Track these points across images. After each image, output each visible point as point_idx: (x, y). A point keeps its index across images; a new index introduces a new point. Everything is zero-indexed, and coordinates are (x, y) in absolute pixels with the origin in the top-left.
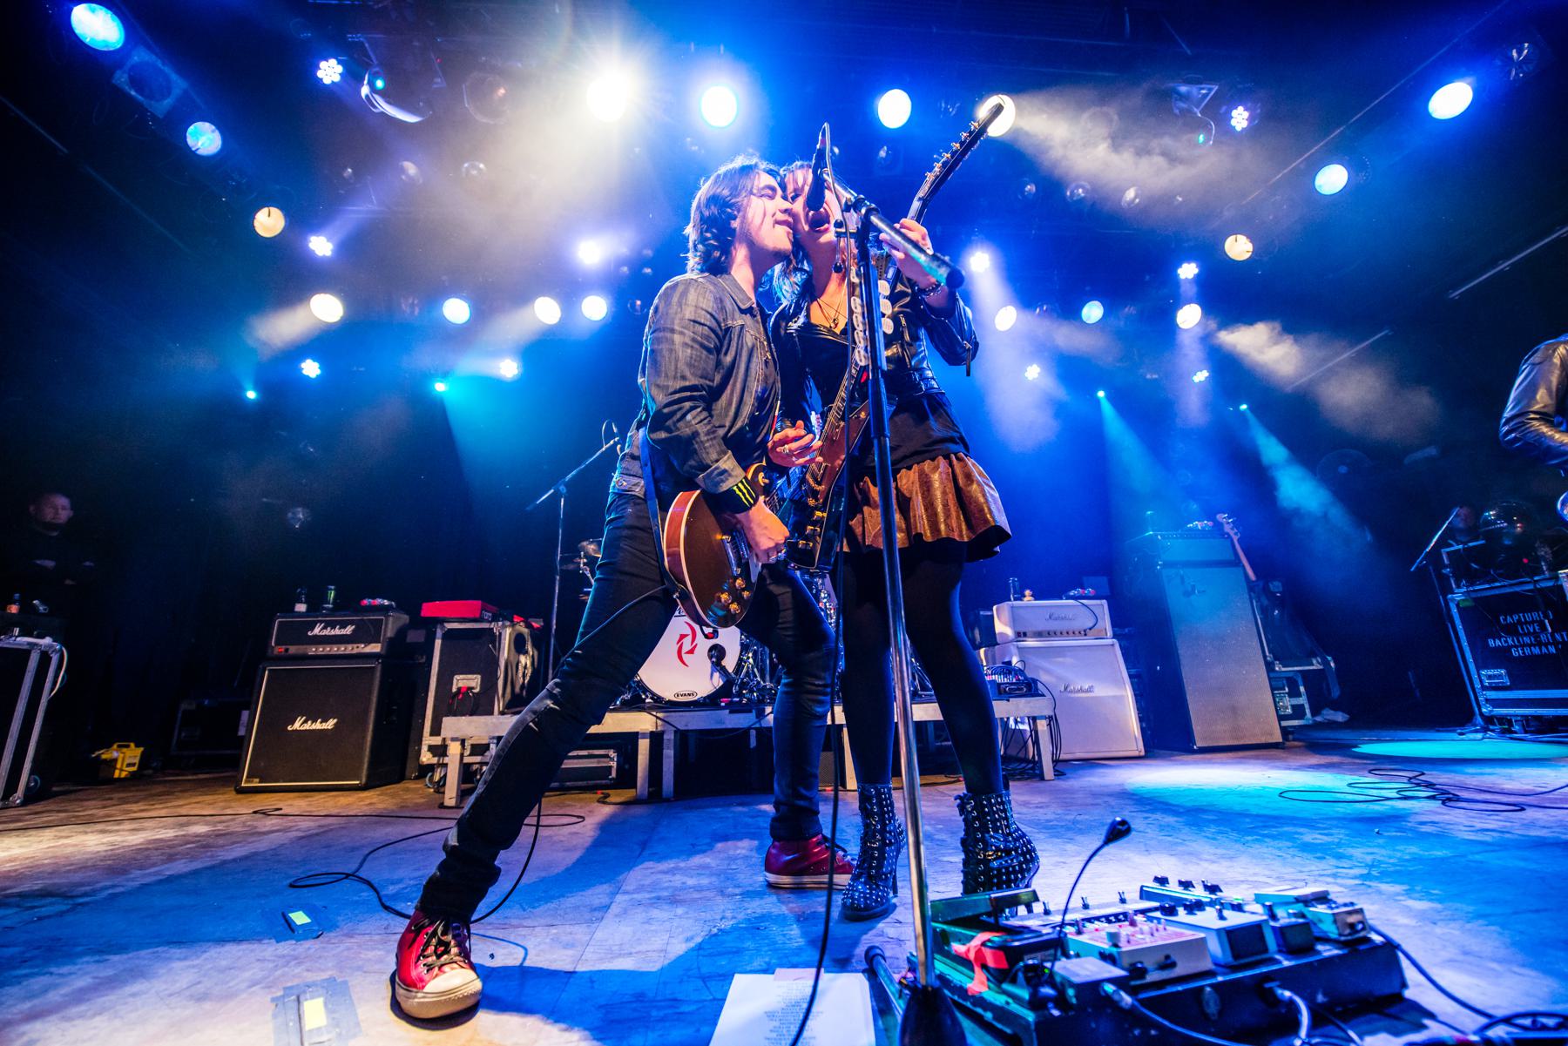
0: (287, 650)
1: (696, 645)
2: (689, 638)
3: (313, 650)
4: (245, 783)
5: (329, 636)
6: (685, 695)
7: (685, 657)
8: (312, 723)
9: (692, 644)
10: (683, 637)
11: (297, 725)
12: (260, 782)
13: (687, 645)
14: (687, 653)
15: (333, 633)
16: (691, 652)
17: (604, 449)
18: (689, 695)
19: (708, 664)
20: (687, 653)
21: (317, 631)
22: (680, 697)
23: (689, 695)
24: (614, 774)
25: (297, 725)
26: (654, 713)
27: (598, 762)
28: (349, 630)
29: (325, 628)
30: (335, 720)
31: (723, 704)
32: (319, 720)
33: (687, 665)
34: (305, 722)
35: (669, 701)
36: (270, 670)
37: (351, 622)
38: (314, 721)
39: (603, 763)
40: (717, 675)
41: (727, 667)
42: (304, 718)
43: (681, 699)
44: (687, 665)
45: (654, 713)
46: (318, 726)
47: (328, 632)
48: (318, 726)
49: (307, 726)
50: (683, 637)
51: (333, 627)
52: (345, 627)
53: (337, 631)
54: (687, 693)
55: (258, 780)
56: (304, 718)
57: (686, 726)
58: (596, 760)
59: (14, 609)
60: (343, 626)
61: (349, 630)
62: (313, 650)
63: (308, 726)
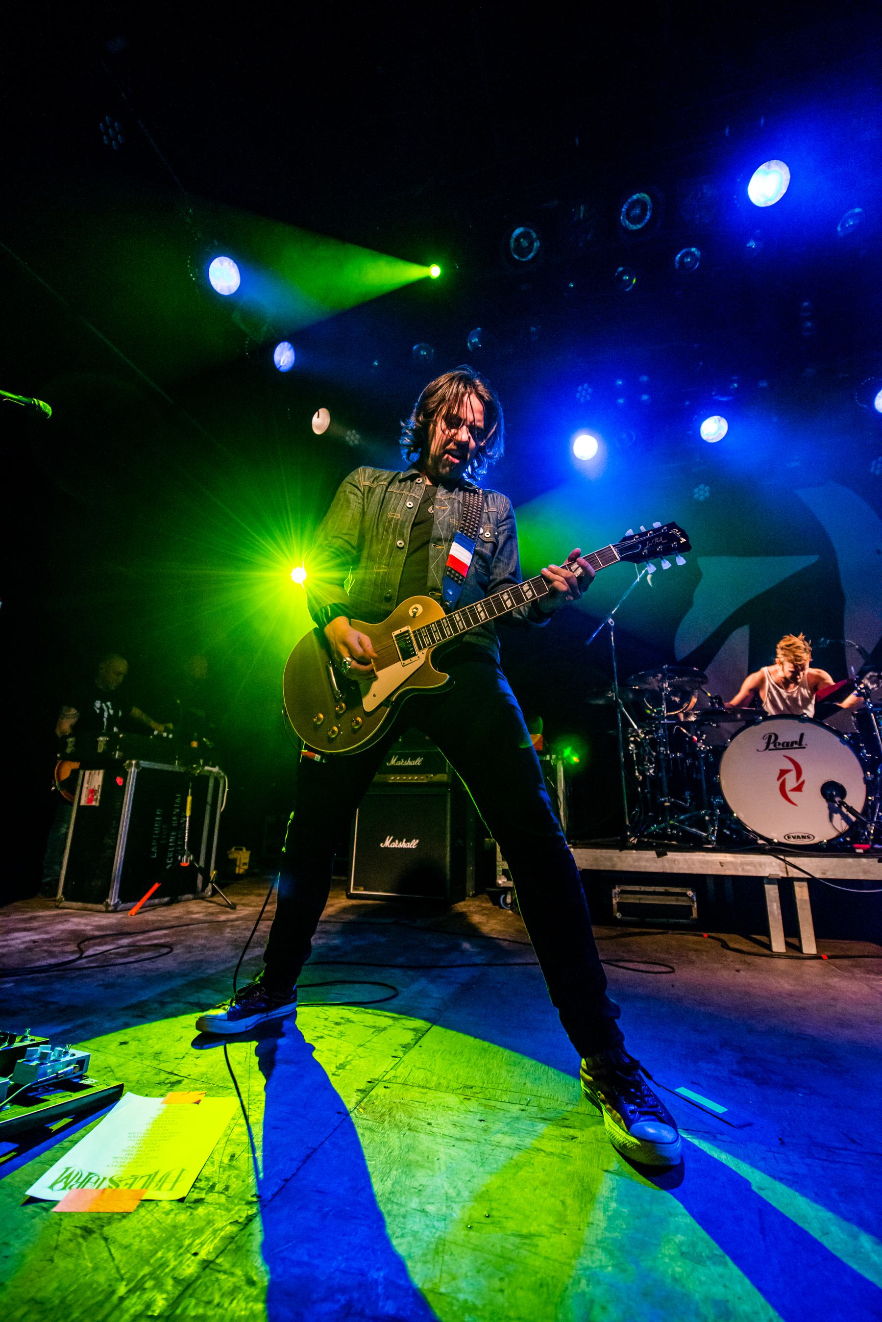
3: (392, 778)
4: (355, 889)
6: (798, 837)
7: (792, 795)
8: (399, 842)
10: (783, 772)
11: (387, 843)
12: (365, 890)
13: (791, 781)
14: (794, 790)
16: (799, 789)
17: (638, 580)
18: (804, 837)
19: (823, 804)
21: (393, 762)
22: (792, 839)
23: (804, 837)
24: (695, 914)
25: (387, 843)
26: (782, 857)
27: (677, 900)
28: (418, 762)
29: (399, 760)
31: (860, 851)
32: (405, 840)
34: (393, 841)
35: (780, 844)
38: (401, 840)
39: (682, 902)
40: (837, 817)
41: (854, 807)
43: (792, 841)
45: (782, 857)
46: (403, 845)
47: (401, 763)
48: (403, 845)
49: (395, 845)
50: (783, 772)
51: (406, 759)
52: (415, 759)
53: (409, 763)
54: (800, 835)
55: (362, 888)
57: (824, 873)
58: (673, 898)
59: (195, 744)
60: (414, 758)
61: (418, 762)
62: (392, 778)
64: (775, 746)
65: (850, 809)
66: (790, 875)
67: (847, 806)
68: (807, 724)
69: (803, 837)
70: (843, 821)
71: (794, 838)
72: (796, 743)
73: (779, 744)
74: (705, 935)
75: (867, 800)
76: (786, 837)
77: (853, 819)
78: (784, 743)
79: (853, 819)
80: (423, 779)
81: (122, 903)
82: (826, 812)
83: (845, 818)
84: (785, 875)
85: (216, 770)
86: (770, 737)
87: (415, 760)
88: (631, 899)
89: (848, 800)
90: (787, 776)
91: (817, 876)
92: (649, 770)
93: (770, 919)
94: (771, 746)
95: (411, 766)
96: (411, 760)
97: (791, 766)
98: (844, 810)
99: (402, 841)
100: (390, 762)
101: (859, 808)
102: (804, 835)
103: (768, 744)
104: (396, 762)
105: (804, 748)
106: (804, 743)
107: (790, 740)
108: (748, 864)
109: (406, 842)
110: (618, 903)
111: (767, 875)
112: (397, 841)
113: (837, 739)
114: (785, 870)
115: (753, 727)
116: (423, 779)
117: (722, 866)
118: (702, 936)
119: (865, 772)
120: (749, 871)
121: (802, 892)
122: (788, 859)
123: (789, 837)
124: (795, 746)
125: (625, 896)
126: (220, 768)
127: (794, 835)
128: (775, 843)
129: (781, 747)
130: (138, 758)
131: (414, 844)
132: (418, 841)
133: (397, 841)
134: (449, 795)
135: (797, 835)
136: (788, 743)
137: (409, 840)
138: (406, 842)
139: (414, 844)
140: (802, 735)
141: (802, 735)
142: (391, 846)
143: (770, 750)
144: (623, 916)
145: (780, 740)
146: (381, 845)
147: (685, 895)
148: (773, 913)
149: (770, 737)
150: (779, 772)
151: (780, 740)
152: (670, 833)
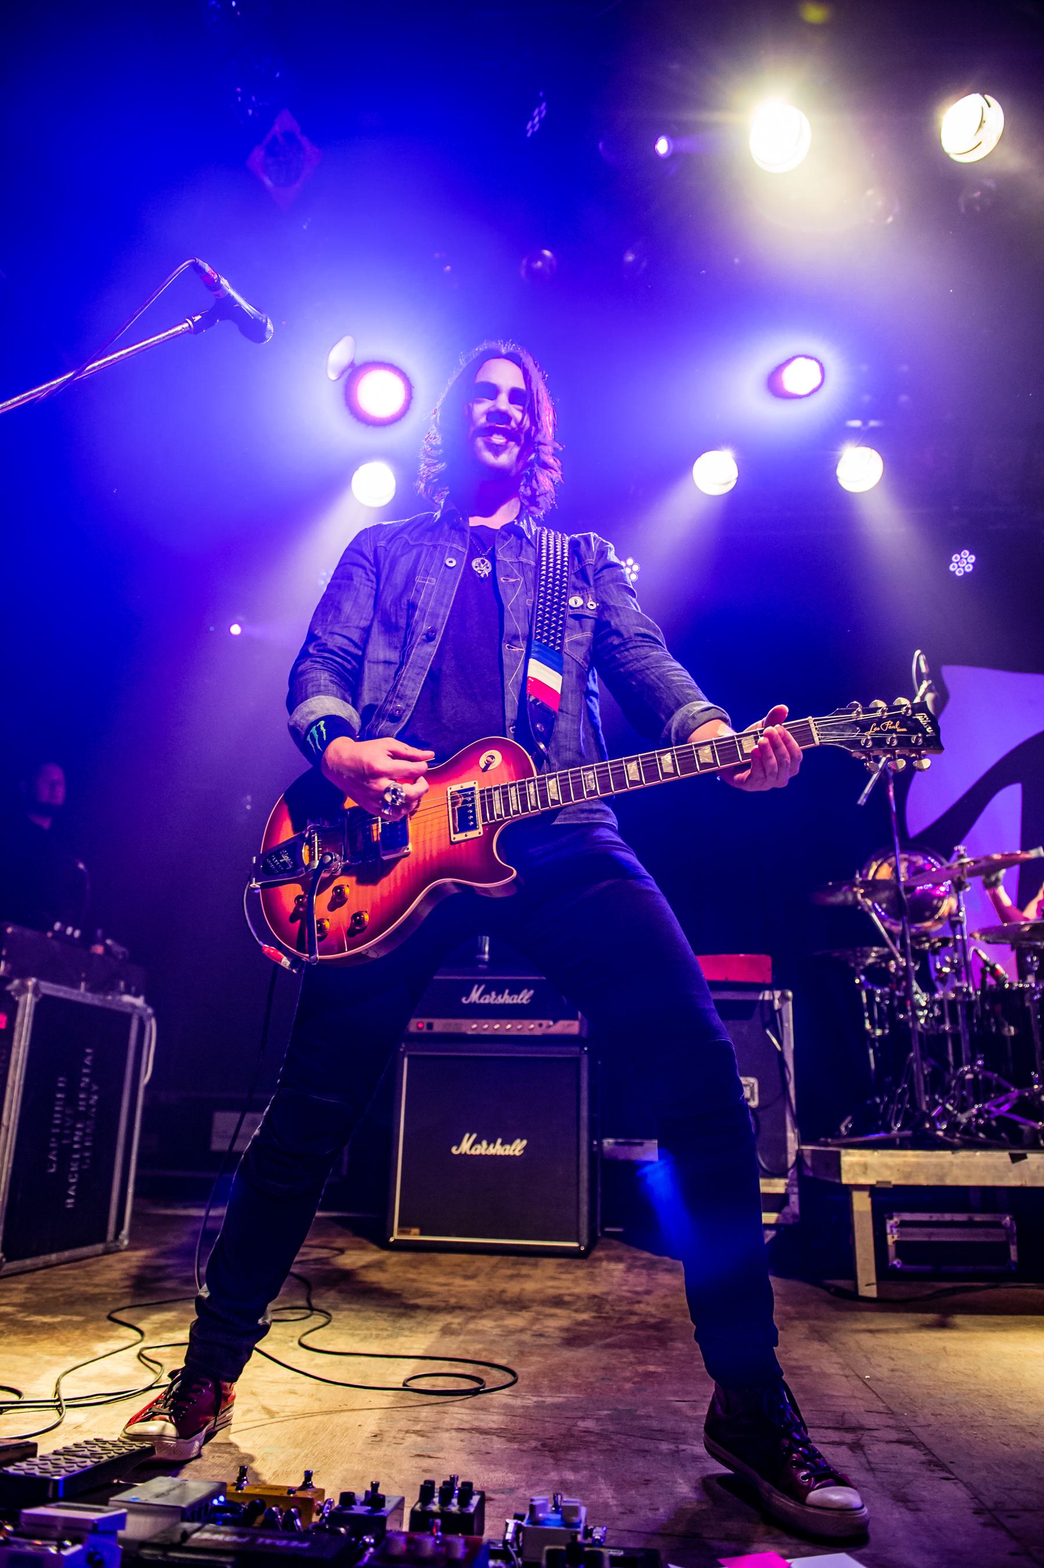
0: (430, 1026)
3: (472, 1027)
4: (401, 1232)
5: (495, 1005)
11: (465, 1146)
12: (422, 1234)
15: (500, 1000)
21: (475, 996)
25: (465, 1146)
28: (524, 997)
30: (525, 1142)
34: (477, 1142)
36: (409, 1057)
37: (528, 985)
38: (491, 1141)
39: (995, 1236)
42: (474, 1136)
46: (498, 1149)
47: (491, 999)
48: (498, 1149)
49: (482, 1149)
51: (500, 992)
53: (506, 999)
55: (416, 1231)
56: (474, 1136)
60: (515, 991)
61: (524, 997)
62: (472, 1027)
63: (483, 1149)
80: (532, 1027)
81: (8, 1261)
85: (139, 1002)
87: (519, 993)
88: (918, 1236)
95: (509, 1005)
96: (510, 994)
99: (495, 1143)
100: (468, 996)
104: (480, 998)
109: (502, 1144)
110: (896, 1242)
112: (484, 1143)
116: (532, 1027)
125: (910, 1230)
126: (147, 1001)
130: (40, 976)
131: (517, 1148)
132: (525, 1142)
133: (484, 1143)
134: (585, 1061)
137: (508, 1141)
138: (502, 1144)
139: (517, 1148)
142: (473, 1152)
144: (904, 1262)
146: (454, 1150)
147: (998, 1225)
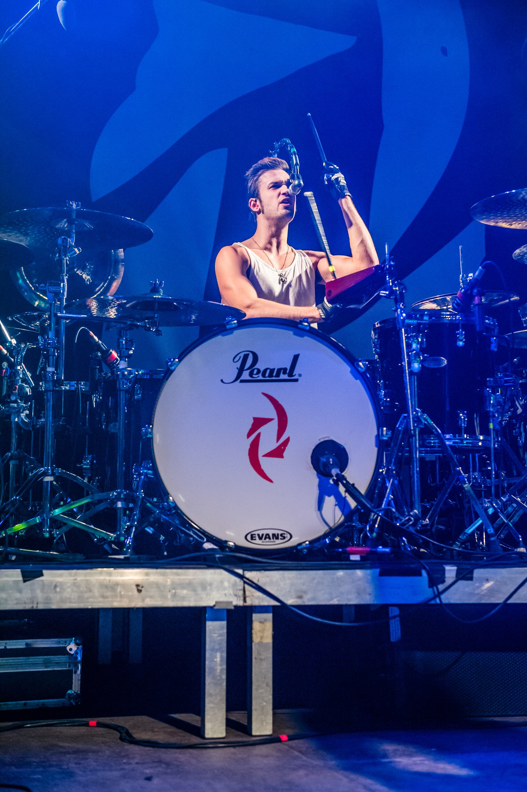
1: (288, 440)
2: (273, 427)
6: (267, 536)
7: (265, 463)
9: (278, 439)
14: (270, 455)
20: (270, 455)
22: (258, 541)
24: (76, 687)
26: (240, 571)
27: (46, 664)
31: (355, 558)
33: (271, 481)
35: (238, 549)
40: (330, 501)
43: (258, 544)
44: (271, 481)
45: (240, 571)
54: (271, 532)
57: (300, 597)
58: (40, 659)
64: (251, 374)
65: (351, 489)
66: (249, 602)
67: (347, 482)
68: (306, 338)
69: (274, 535)
70: (337, 508)
71: (260, 538)
72: (285, 369)
73: (259, 371)
74: (93, 721)
75: (376, 474)
76: (249, 537)
77: (353, 504)
78: (265, 371)
79: (353, 504)
82: (315, 492)
83: (342, 503)
84: (241, 603)
86: (246, 357)
89: (350, 474)
90: (263, 430)
91: (290, 601)
92: (18, 413)
93: (208, 680)
94: (246, 375)
97: (271, 413)
98: (342, 489)
101: (363, 488)
102: (276, 532)
103: (241, 371)
105: (296, 380)
106: (296, 372)
107: (276, 365)
108: (183, 586)
111: (212, 604)
113: (346, 368)
114: (241, 593)
115: (219, 338)
117: (139, 591)
118: (87, 725)
119: (380, 426)
120: (183, 598)
121: (262, 631)
122: (249, 575)
123: (252, 537)
124: (282, 376)
127: (260, 533)
128: (230, 548)
129: (261, 377)
135: (265, 532)
136: (272, 371)
140: (296, 358)
141: (296, 358)
143: (242, 381)
145: (261, 366)
147: (63, 651)
148: (213, 669)
149: (246, 357)
150: (252, 421)
151: (261, 366)
152: (47, 535)
